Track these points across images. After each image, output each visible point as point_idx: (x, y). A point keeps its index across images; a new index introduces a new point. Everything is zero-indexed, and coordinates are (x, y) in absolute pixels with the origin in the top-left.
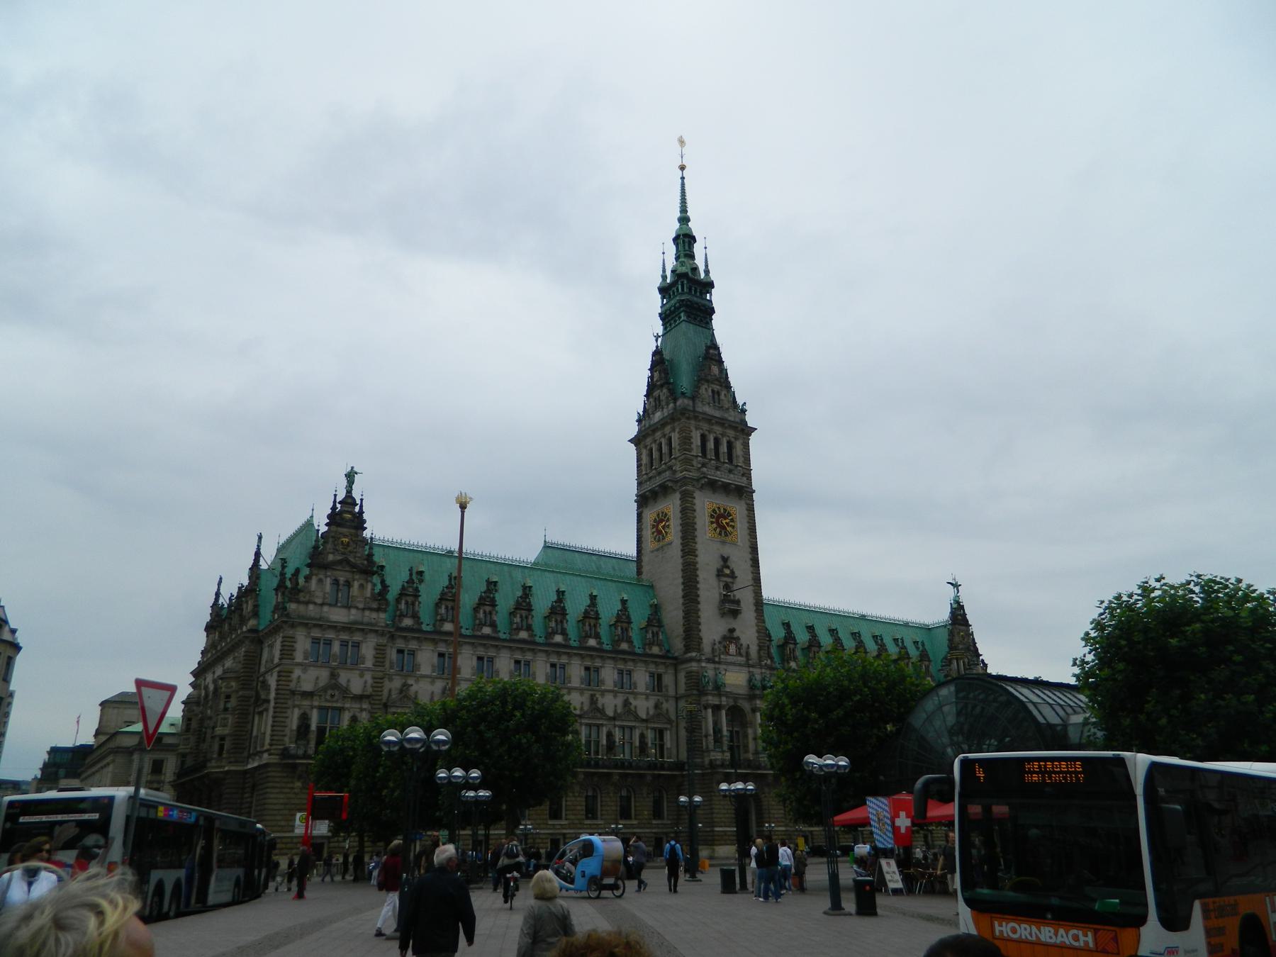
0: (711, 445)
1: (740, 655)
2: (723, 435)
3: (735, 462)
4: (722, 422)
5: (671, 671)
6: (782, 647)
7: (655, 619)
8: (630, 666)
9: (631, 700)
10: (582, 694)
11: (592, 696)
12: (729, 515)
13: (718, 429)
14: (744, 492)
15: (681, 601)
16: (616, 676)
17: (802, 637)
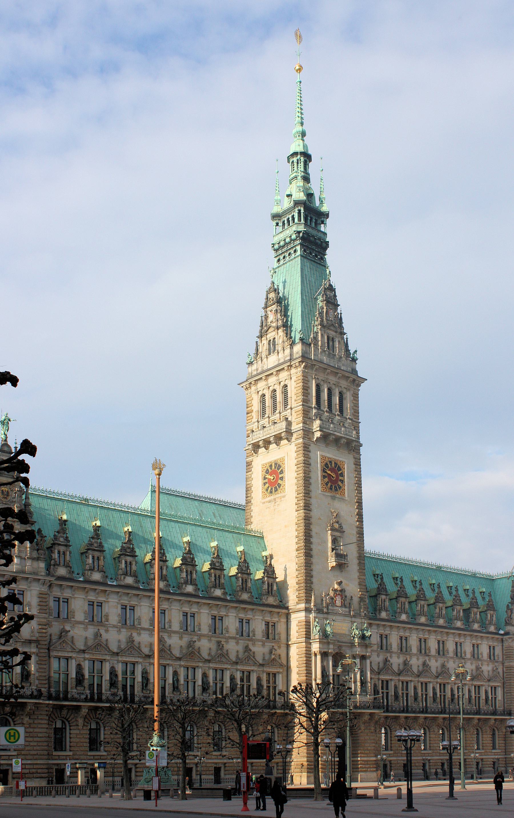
0: (325, 395)
1: (343, 605)
2: (337, 385)
3: (344, 415)
4: (335, 372)
5: (284, 620)
6: (375, 597)
7: (270, 571)
8: (249, 616)
9: (251, 647)
10: (210, 640)
11: (219, 643)
12: (339, 469)
13: (332, 379)
14: (353, 447)
15: (295, 553)
16: (237, 624)
17: (391, 588)
